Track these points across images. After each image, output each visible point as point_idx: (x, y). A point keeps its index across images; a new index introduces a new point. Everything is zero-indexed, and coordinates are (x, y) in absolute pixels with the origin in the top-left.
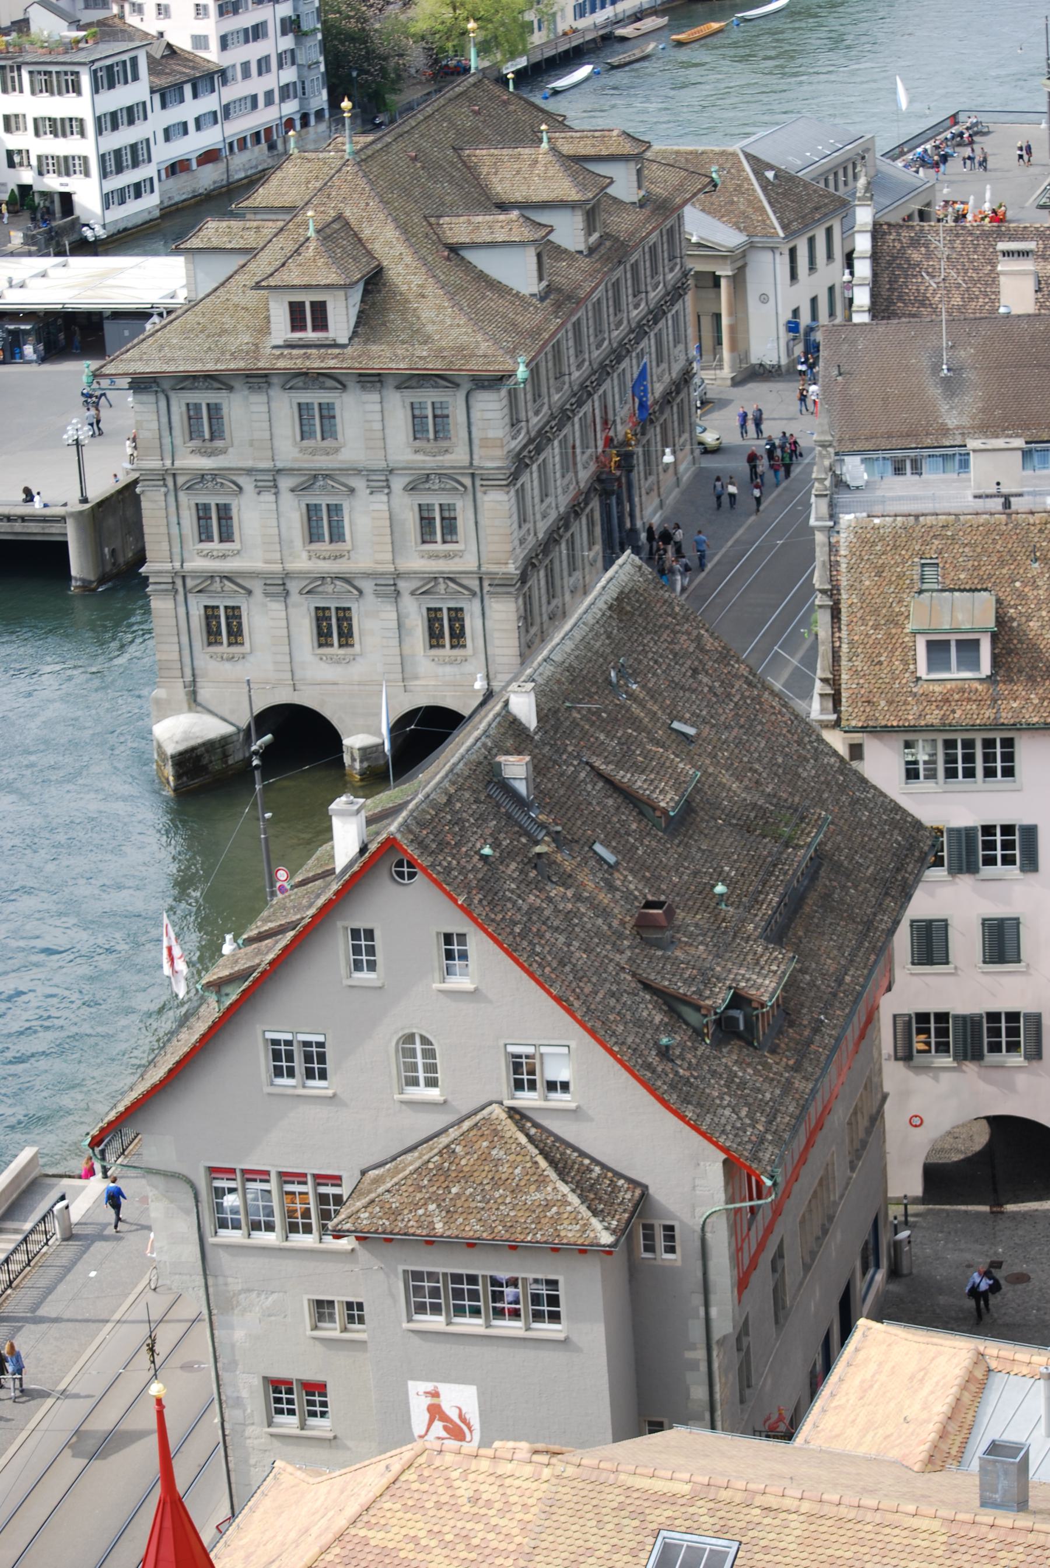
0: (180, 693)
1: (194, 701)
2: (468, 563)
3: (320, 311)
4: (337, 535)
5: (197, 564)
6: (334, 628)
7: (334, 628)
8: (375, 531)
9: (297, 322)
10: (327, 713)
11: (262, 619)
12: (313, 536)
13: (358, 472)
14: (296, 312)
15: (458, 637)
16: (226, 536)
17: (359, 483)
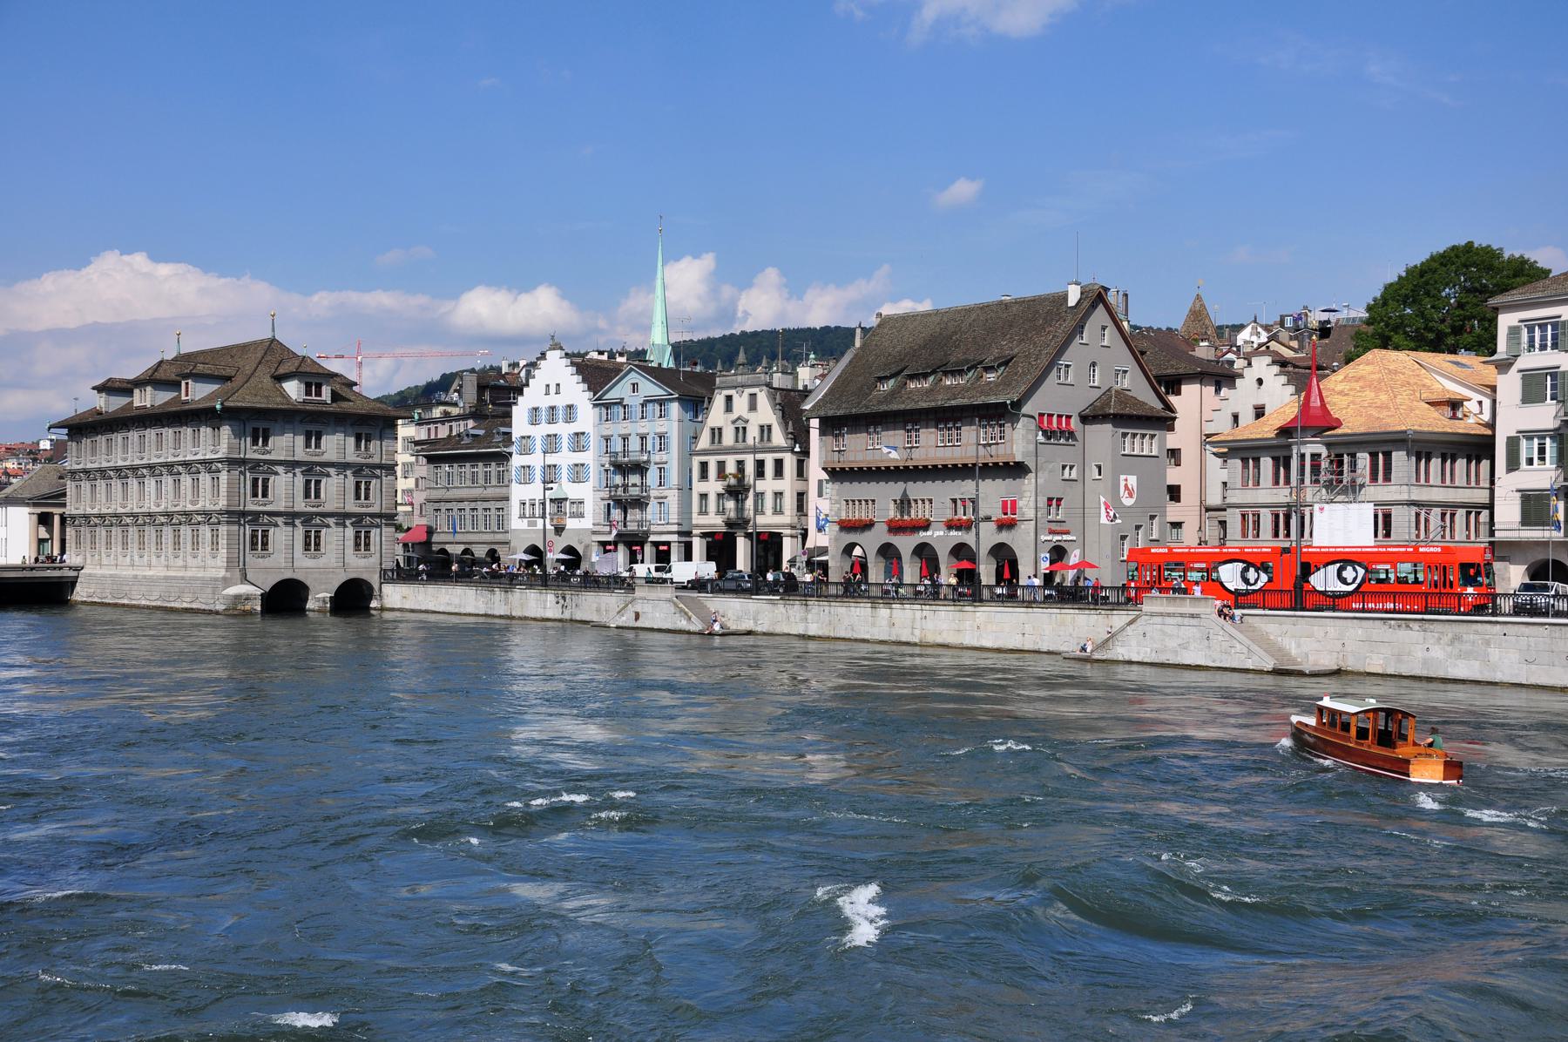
0: (237, 574)
1: (245, 579)
2: (375, 509)
3: (319, 387)
4: (317, 496)
5: (251, 507)
6: (312, 543)
7: (312, 543)
8: (335, 491)
9: (308, 393)
10: (308, 583)
11: (280, 536)
12: (307, 495)
13: (332, 465)
14: (308, 386)
15: (367, 545)
16: (265, 495)
17: (332, 471)
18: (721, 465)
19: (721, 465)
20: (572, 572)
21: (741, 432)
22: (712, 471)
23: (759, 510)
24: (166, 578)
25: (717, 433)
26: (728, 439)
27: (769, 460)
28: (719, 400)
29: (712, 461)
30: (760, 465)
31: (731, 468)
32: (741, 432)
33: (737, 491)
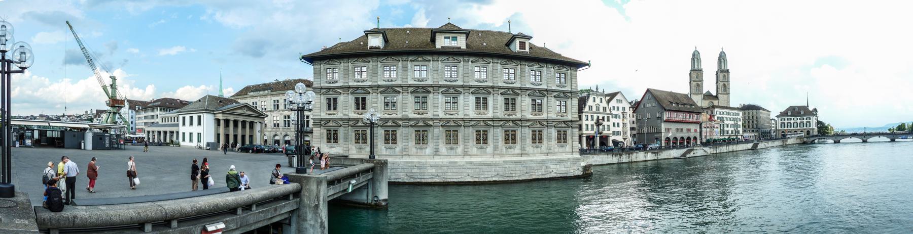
18: (592, 117)
19: (592, 117)
20: (619, 149)
21: (598, 108)
22: (590, 118)
23: (604, 129)
24: (505, 162)
25: (591, 107)
26: (594, 109)
27: (606, 116)
28: (591, 98)
29: (589, 115)
30: (603, 118)
31: (595, 118)
32: (598, 108)
33: (598, 124)
